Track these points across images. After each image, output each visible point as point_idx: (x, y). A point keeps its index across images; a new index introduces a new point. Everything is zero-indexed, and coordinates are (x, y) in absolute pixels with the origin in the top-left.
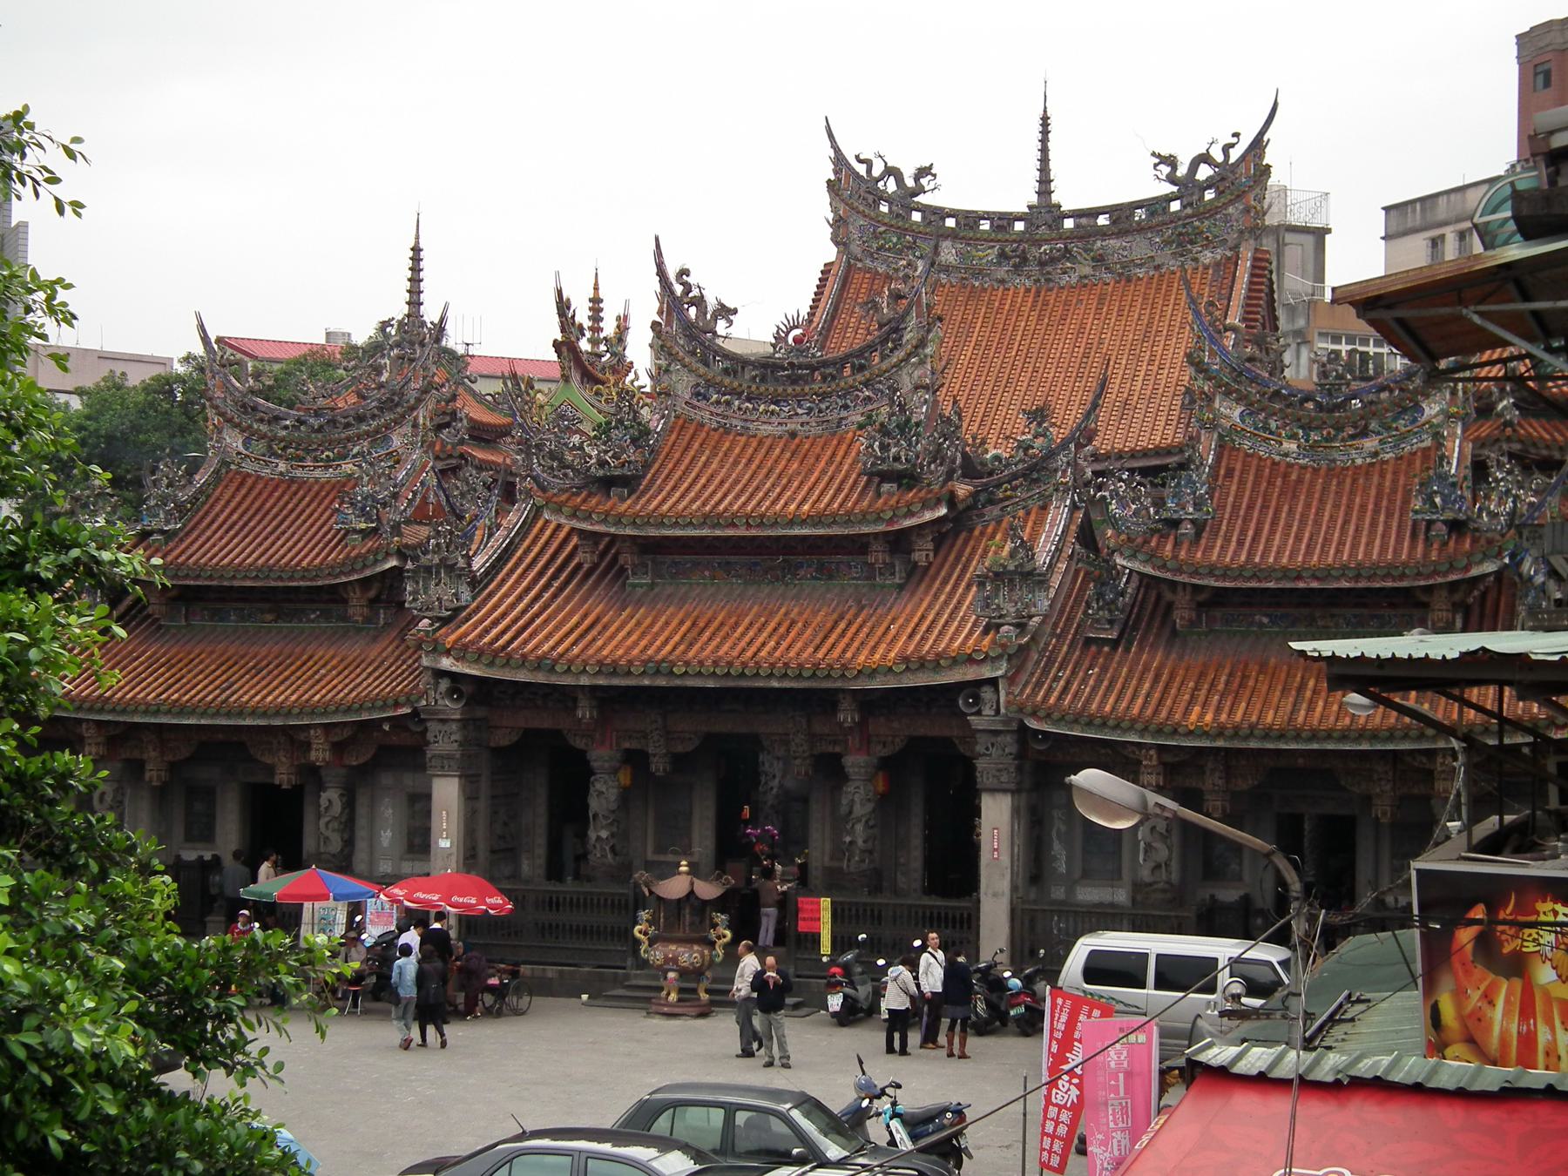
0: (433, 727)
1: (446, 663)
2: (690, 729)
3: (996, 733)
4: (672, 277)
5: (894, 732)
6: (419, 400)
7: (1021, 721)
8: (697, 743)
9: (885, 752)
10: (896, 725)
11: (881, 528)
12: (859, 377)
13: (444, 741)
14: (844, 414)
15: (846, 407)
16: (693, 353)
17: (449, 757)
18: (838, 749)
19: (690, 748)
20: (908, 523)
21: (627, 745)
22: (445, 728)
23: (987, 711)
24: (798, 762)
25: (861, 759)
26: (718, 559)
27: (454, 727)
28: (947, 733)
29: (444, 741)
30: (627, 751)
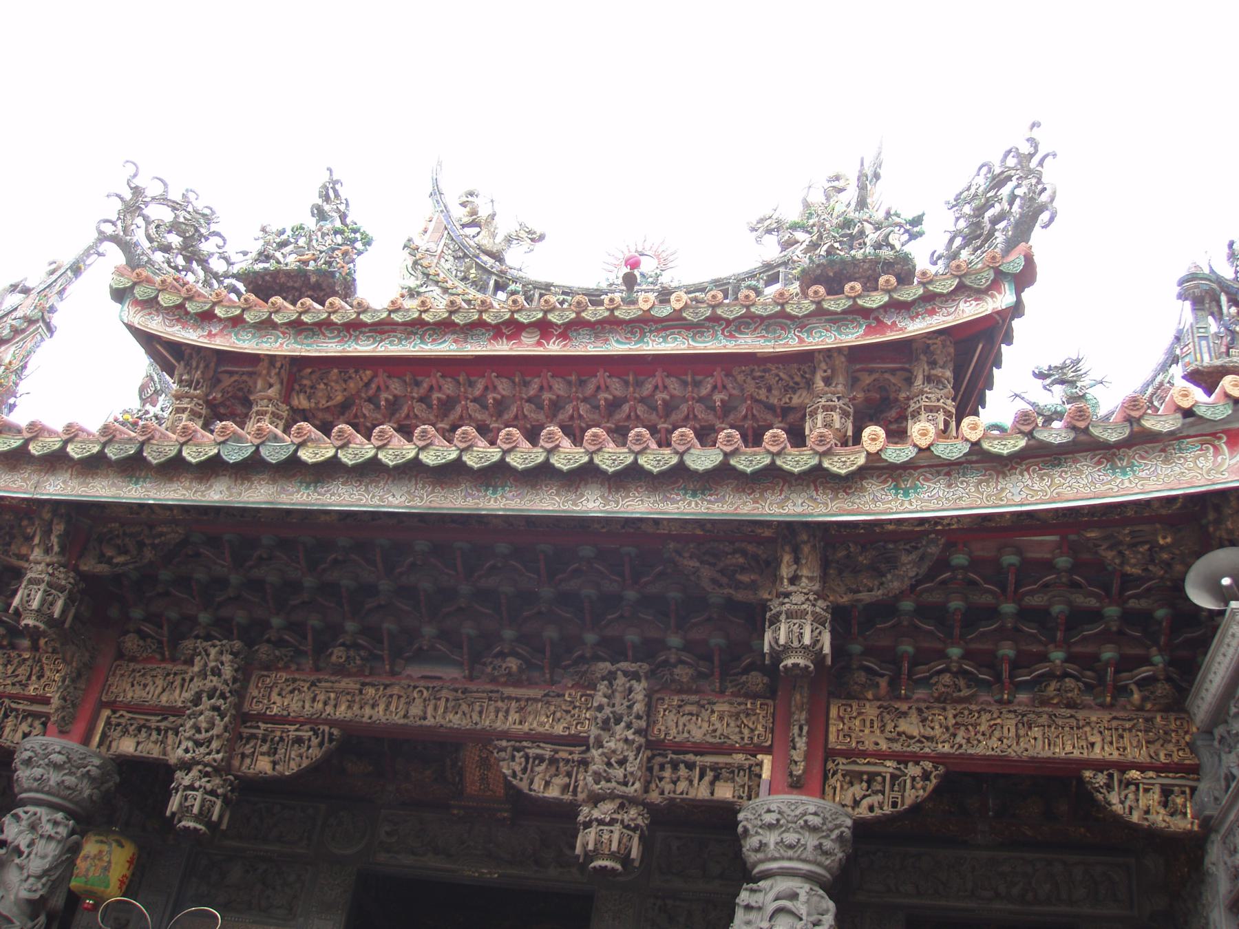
2: (309, 708)
4: (452, 200)
5: (914, 739)
6: (16, 331)
8: (315, 753)
9: (874, 806)
10: (910, 726)
11: (853, 336)
16: (465, 279)
18: (725, 792)
19: (293, 762)
20: (915, 327)
21: (127, 746)
24: (605, 810)
25: (809, 804)
28: (1067, 748)
30: (125, 764)
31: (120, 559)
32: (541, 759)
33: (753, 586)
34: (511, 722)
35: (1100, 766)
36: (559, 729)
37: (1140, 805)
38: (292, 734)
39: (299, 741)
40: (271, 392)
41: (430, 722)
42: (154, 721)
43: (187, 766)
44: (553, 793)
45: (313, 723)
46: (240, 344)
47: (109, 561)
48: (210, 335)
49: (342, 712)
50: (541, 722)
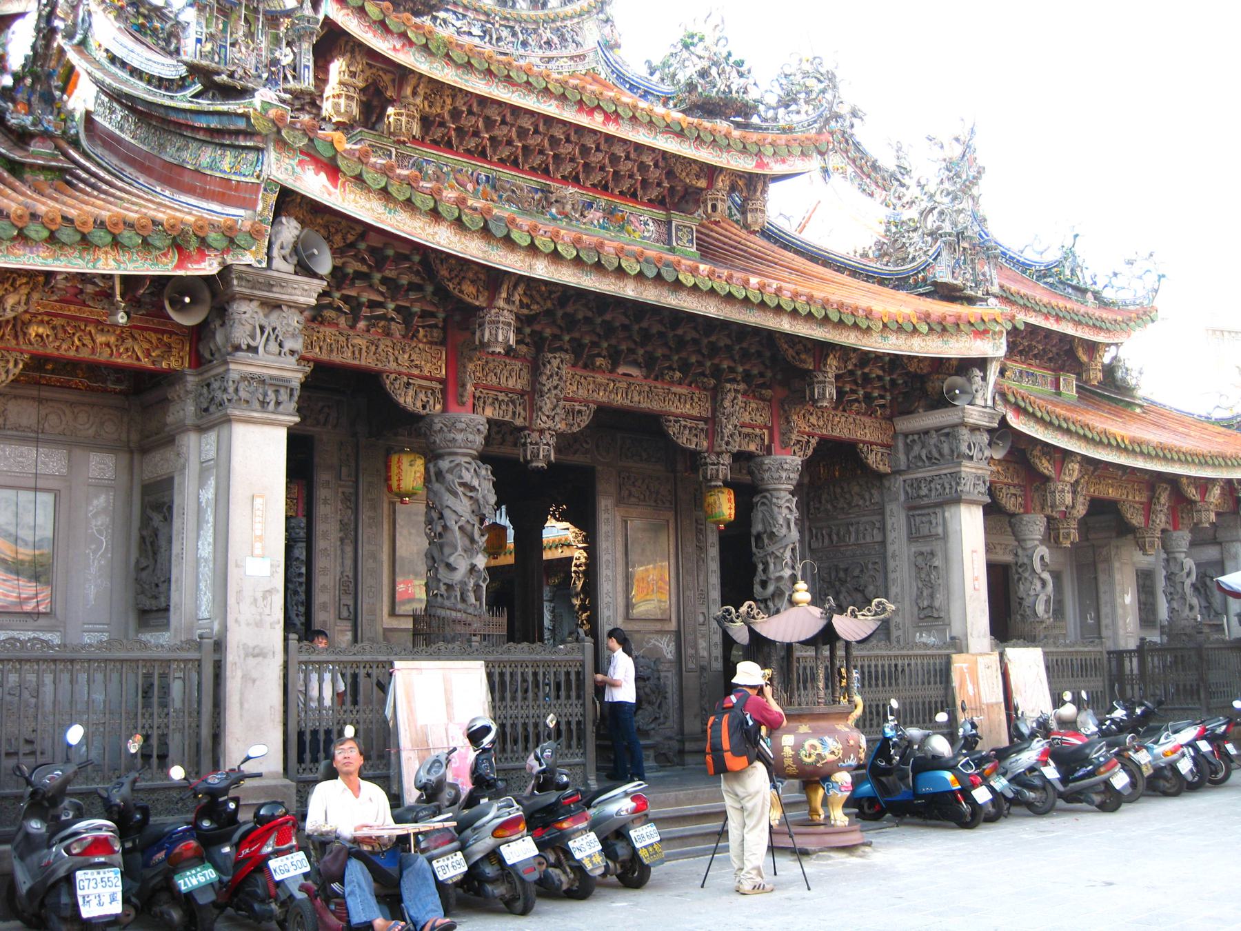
0: (246, 314)
1: (314, 184)
3: (975, 429)
7: (1003, 420)
10: (813, 420)
12: (540, 13)
13: (269, 348)
14: (521, 51)
15: (525, 44)
17: (278, 385)
18: (752, 447)
22: (274, 319)
23: (979, 401)
26: (484, 169)
27: (294, 320)
28: (858, 435)
29: (269, 348)
31: (535, 307)
32: (685, 427)
33: (804, 362)
34: (673, 410)
35: (865, 443)
36: (695, 413)
37: (875, 460)
38: (577, 408)
39: (580, 412)
40: (418, 101)
41: (643, 405)
42: (501, 396)
43: (542, 431)
44: (693, 446)
45: (586, 402)
46: (418, 65)
47: (528, 306)
48: (394, 49)
49: (601, 397)
50: (687, 409)
